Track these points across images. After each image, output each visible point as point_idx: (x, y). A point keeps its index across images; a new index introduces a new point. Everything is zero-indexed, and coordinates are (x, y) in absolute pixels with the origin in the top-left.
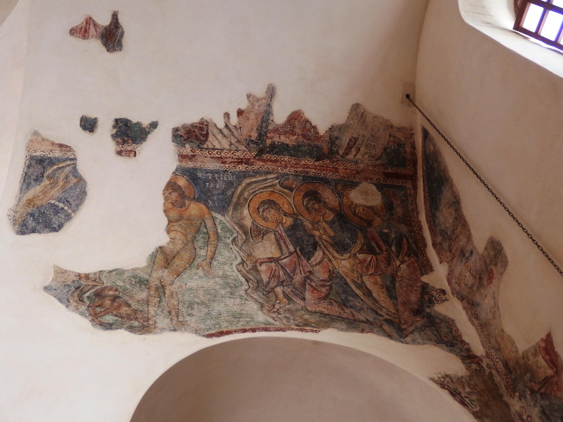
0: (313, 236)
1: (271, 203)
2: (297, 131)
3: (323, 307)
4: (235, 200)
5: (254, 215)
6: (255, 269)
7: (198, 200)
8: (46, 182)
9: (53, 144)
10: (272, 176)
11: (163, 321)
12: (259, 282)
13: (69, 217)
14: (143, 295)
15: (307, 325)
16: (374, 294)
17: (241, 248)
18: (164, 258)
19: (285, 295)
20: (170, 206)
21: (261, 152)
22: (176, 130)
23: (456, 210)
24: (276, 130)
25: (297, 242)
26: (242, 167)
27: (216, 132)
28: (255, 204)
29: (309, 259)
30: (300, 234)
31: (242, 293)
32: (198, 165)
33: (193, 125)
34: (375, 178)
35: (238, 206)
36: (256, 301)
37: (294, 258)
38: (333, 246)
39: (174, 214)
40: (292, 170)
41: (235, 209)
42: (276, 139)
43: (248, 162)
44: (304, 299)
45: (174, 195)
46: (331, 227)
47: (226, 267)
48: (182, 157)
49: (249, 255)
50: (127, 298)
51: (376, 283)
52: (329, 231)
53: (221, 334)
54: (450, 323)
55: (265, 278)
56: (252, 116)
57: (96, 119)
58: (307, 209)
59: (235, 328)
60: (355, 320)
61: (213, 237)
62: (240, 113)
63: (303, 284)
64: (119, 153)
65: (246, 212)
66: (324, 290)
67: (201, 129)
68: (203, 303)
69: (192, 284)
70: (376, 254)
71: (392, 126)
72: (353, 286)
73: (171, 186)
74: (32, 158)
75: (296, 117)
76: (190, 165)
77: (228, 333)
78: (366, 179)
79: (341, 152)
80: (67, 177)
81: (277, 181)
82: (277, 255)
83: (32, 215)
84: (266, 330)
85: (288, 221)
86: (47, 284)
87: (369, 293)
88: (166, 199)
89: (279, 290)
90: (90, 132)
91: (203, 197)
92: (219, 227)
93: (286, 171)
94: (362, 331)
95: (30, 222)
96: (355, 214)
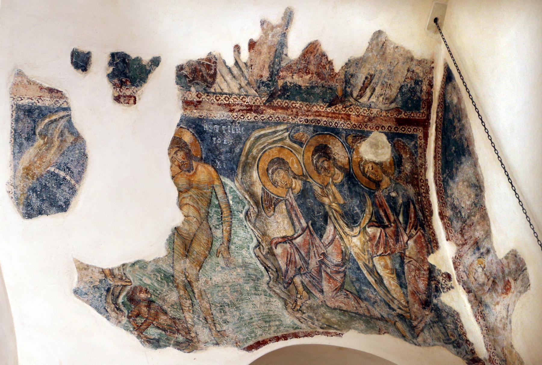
0: (322, 204)
1: (280, 162)
2: (312, 68)
3: (340, 301)
4: (243, 159)
5: (264, 179)
6: (271, 252)
7: (205, 160)
8: (40, 141)
9: (41, 88)
10: (282, 127)
11: (203, 333)
12: (278, 270)
13: (73, 191)
14: (173, 297)
15: (330, 327)
16: (385, 282)
17: (254, 226)
18: (182, 242)
19: (305, 287)
20: (177, 170)
21: (272, 96)
22: (180, 68)
23: (477, 195)
24: (289, 68)
25: (309, 213)
26: (251, 116)
27: (225, 71)
28: (263, 165)
29: (321, 236)
30: (310, 202)
31: (265, 286)
32: (204, 114)
33: (199, 62)
34: (387, 125)
35: (247, 167)
36: (280, 297)
37: (306, 236)
38: (342, 216)
39: (183, 181)
40: (304, 118)
41: (244, 171)
42: (289, 79)
43: (256, 109)
44: (322, 291)
45: (180, 155)
46: (340, 192)
47: (244, 252)
48: (187, 103)
49: (264, 234)
50: (160, 302)
51: (386, 267)
52: (338, 196)
53: (259, 344)
54: (455, 316)
55: (282, 263)
56: (265, 49)
57: (89, 53)
58: (317, 169)
59: (269, 336)
60: (371, 317)
61: (226, 213)
62: (252, 45)
63: (319, 272)
64: (117, 99)
65: (255, 174)
66: (339, 277)
67: (208, 67)
68: (232, 305)
69: (217, 278)
70: (385, 227)
71: (412, 59)
72: (365, 272)
73: (177, 143)
74: (19, 108)
75: (312, 49)
76: (195, 114)
77: (264, 343)
78: (377, 128)
79: (355, 94)
80: (62, 134)
81: (287, 134)
82: (290, 233)
83: (34, 190)
84: (296, 336)
85: (298, 185)
86: (75, 286)
87: (380, 280)
88: (172, 160)
89: (297, 280)
90: (83, 71)
91: (210, 158)
92: (230, 198)
93: (297, 120)
94: (380, 332)
95: (34, 200)
96: (364, 173)
